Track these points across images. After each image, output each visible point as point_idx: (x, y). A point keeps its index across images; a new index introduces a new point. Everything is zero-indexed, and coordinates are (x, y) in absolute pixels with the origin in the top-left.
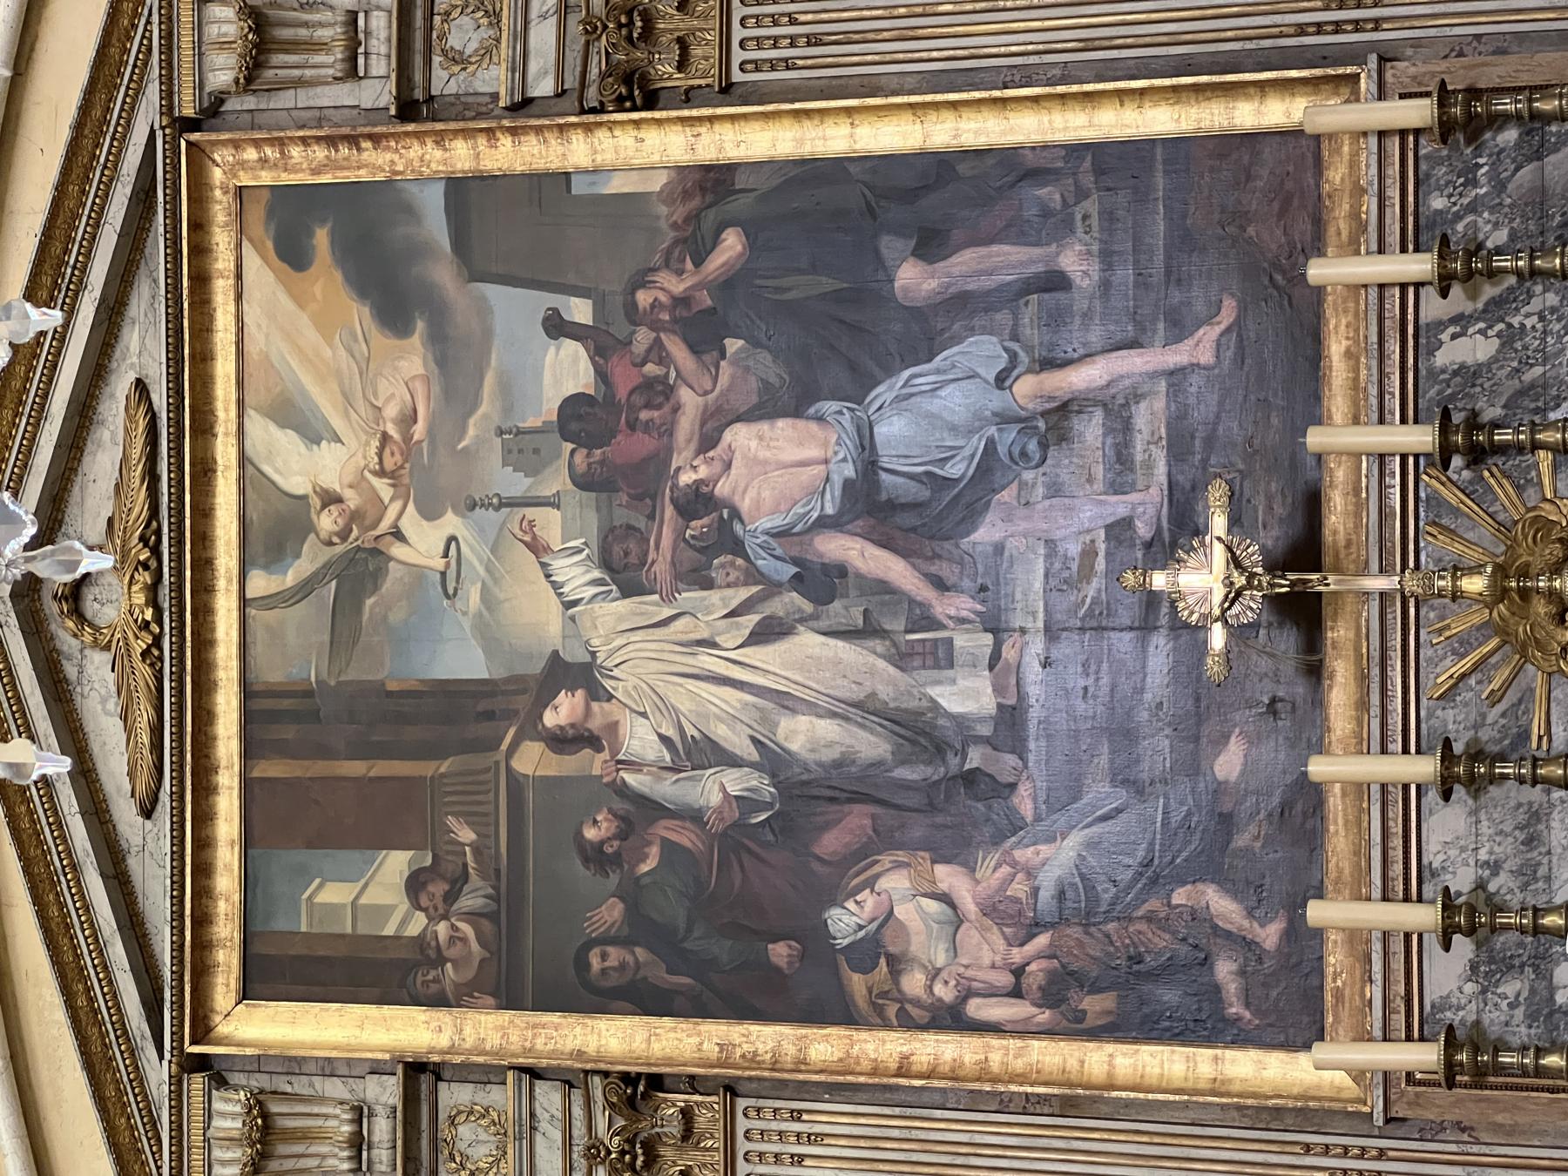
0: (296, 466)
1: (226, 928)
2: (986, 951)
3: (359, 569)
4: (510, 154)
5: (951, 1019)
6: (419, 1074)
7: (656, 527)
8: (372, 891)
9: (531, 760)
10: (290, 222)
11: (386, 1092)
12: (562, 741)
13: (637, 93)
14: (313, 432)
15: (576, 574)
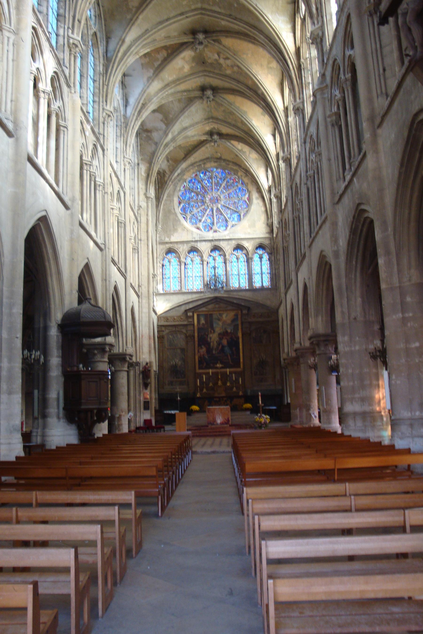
0: (224, 316)
1: (200, 313)
2: (202, 353)
3: (219, 320)
4: (240, 327)
5: (198, 351)
6: (194, 325)
7: (222, 335)
8: (203, 321)
9: (210, 329)
10: (236, 315)
11: (192, 323)
12: (211, 332)
13: (243, 335)
14: (226, 317)
15: (219, 332)
